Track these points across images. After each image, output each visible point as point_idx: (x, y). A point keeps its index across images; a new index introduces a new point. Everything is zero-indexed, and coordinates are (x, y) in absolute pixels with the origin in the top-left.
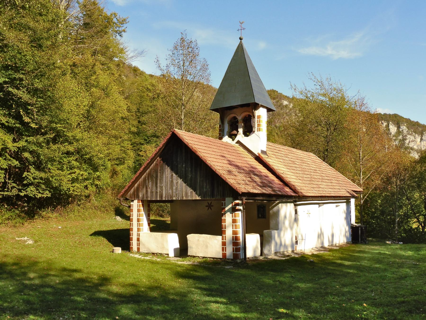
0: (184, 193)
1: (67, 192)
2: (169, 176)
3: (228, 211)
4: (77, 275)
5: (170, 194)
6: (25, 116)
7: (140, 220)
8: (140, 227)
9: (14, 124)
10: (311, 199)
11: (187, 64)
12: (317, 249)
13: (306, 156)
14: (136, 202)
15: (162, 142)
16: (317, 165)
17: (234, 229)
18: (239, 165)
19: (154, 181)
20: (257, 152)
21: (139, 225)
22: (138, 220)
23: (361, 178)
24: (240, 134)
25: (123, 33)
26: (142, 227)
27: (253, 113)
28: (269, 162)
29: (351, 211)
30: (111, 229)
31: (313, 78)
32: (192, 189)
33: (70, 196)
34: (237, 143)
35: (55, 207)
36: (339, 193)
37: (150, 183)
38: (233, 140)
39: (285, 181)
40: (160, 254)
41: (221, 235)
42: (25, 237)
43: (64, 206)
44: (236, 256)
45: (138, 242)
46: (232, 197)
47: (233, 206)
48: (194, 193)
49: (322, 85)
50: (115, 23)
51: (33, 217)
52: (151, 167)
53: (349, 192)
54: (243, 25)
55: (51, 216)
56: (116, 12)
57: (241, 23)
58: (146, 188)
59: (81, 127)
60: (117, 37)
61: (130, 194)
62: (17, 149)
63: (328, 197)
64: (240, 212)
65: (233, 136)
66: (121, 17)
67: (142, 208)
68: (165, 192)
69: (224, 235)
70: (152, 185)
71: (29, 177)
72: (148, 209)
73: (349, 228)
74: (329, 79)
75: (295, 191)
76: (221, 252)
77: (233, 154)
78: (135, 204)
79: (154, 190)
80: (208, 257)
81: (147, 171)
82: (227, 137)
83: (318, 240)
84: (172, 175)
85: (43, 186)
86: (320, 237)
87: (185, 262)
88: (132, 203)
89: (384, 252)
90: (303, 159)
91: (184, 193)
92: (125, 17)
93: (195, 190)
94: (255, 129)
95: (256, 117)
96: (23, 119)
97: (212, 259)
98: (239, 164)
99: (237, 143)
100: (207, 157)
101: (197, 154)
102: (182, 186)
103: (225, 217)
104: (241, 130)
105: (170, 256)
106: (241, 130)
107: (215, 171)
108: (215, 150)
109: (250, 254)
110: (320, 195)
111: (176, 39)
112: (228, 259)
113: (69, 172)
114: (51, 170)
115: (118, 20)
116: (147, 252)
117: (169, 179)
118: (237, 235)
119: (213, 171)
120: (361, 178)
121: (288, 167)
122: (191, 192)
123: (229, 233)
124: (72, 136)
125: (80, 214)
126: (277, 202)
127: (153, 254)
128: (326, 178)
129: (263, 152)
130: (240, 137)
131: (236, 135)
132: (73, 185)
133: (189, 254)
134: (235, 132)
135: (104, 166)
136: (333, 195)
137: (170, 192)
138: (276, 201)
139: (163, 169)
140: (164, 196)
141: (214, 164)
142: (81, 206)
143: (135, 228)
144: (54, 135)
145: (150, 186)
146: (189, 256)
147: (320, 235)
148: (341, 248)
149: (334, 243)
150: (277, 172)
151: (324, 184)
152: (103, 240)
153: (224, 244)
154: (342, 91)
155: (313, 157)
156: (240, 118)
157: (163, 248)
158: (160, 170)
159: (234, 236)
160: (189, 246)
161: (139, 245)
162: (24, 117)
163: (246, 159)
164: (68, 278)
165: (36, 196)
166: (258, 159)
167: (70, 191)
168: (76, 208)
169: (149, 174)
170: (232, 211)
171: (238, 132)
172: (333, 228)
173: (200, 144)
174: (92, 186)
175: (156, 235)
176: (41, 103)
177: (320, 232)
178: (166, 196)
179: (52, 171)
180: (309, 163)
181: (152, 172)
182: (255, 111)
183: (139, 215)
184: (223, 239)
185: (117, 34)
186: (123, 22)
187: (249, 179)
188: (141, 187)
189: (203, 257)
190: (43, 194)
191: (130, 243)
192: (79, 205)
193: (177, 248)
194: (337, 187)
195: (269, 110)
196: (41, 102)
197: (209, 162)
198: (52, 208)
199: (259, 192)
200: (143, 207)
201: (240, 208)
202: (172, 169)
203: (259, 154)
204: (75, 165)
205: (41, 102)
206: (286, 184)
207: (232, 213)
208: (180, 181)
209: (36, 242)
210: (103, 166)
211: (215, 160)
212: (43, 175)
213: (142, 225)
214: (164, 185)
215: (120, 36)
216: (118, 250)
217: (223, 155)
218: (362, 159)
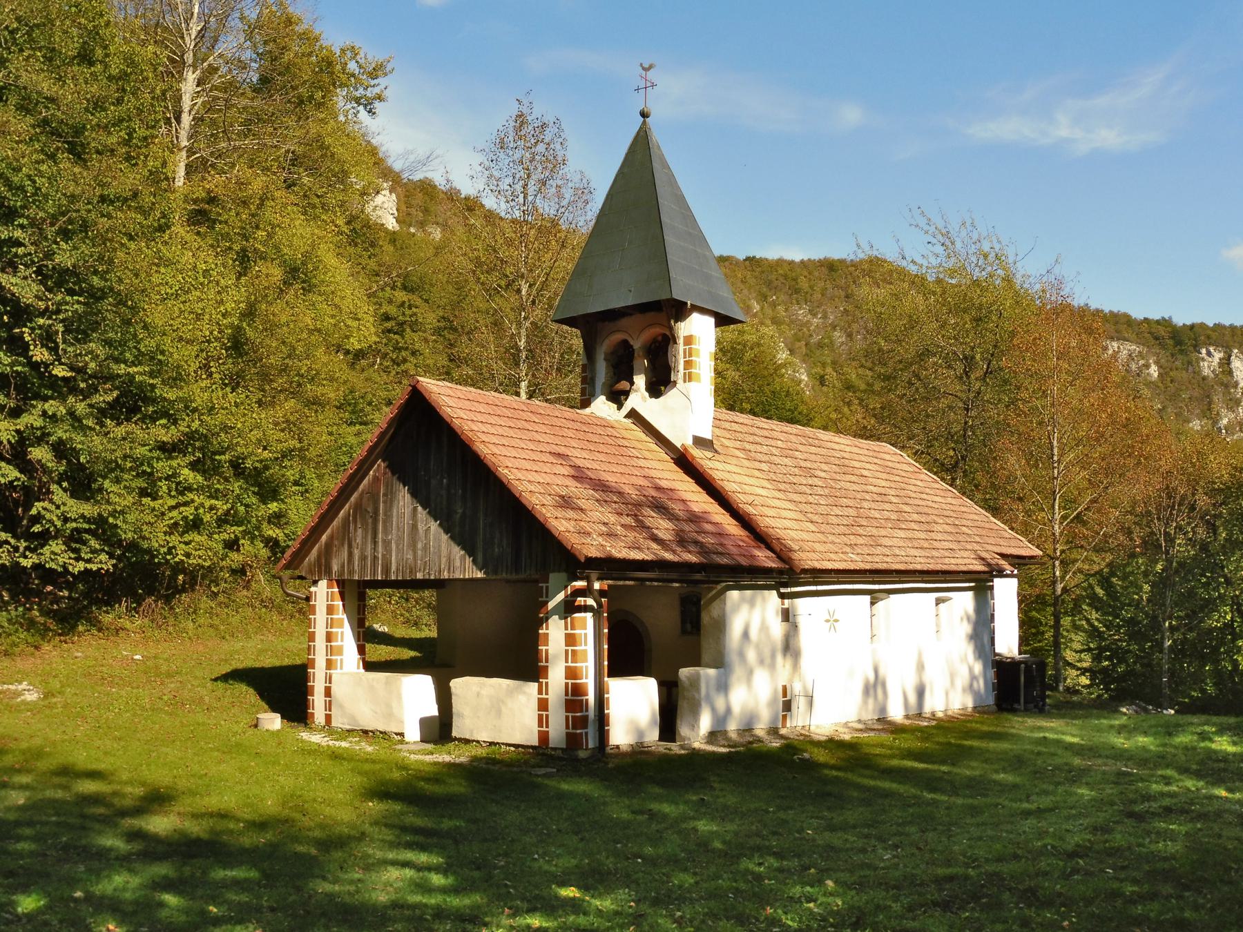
0: (444, 560)
1: (168, 557)
2: (408, 511)
3: (555, 611)
4: (89, 787)
5: (409, 562)
6: (36, 346)
7: (334, 637)
8: (333, 657)
9: (12, 365)
10: (834, 578)
11: (531, 189)
12: (860, 726)
13: (866, 452)
14: (323, 584)
15: (382, 417)
16: (897, 478)
17: (570, 664)
18: (610, 479)
19: (370, 527)
20: (682, 439)
21: (331, 650)
22: (329, 637)
23: (1057, 516)
24: (636, 391)
25: (377, 104)
26: (339, 658)
27: (671, 329)
28: (710, 472)
29: (993, 616)
30: (286, 662)
31: (922, 222)
32: (463, 548)
33: (179, 568)
34: (627, 416)
35: (139, 601)
36: (946, 561)
37: (360, 531)
38: (620, 407)
39: (754, 525)
40: (381, 732)
41: (538, 681)
42: (20, 683)
43: (168, 599)
44: (573, 740)
45: (328, 699)
46: (566, 571)
47: (566, 597)
48: (469, 560)
49: (947, 240)
50: (353, 75)
51: (73, 628)
52: (361, 487)
53: (983, 559)
54: (651, 75)
55: (128, 625)
56: (357, 45)
57: (644, 69)
58: (350, 546)
59: (214, 376)
60: (359, 115)
61: (310, 564)
62: (14, 437)
63: (936, 572)
64: (589, 616)
65: (618, 397)
66: (370, 58)
67: (341, 603)
68: (397, 556)
69: (544, 681)
70: (365, 538)
71: (48, 516)
72: (359, 605)
73: (985, 667)
74: (968, 224)
75: (782, 554)
76: (535, 728)
77: (602, 448)
78: (323, 592)
79: (369, 552)
80: (503, 744)
81: (353, 499)
82: (603, 398)
83: (865, 702)
84: (415, 509)
85: (94, 543)
86: (872, 692)
87: (444, 756)
88: (313, 589)
89: (1056, 736)
90: (847, 462)
91: (444, 560)
92: (380, 58)
93: (470, 550)
94: (679, 375)
95: (681, 341)
96: (31, 353)
97: (512, 749)
98: (610, 479)
99: (627, 416)
100: (501, 458)
101: (475, 448)
102: (440, 540)
103: (547, 629)
104: (640, 381)
105: (407, 739)
106: (640, 381)
107: (517, 495)
108: (538, 437)
109: (620, 737)
110: (868, 567)
111: (502, 118)
112: (552, 748)
113: (172, 502)
114: (111, 495)
115: (360, 67)
116: (348, 727)
117: (407, 519)
118: (578, 681)
119: (514, 496)
120: (1057, 516)
121: (782, 486)
122: (463, 559)
123: (556, 677)
124: (180, 399)
125: (216, 621)
126: (719, 587)
127: (366, 732)
128: (915, 517)
129: (699, 442)
130: (639, 399)
131: (626, 394)
132: (187, 538)
133: (454, 734)
134: (624, 385)
135: (301, 485)
136: (919, 567)
137: (410, 556)
138: (718, 582)
139: (392, 492)
140: (394, 568)
141: (520, 475)
142: (221, 598)
143: (320, 661)
144: (115, 393)
145: (359, 540)
146: (456, 739)
147: (874, 687)
148: (947, 725)
149: (927, 709)
150: (731, 501)
151: (902, 534)
152: (248, 694)
153: (543, 705)
154: (1003, 258)
155: (887, 457)
156: (637, 344)
157: (390, 715)
158: (385, 495)
159: (570, 682)
160: (454, 710)
161: (329, 706)
162: (32, 347)
163: (642, 463)
164: (59, 794)
165: (70, 568)
166: (683, 461)
167: (177, 554)
168: (205, 603)
169: (358, 507)
170: (565, 613)
171: (632, 383)
172: (921, 667)
173: (492, 420)
174: (252, 543)
175: (373, 680)
176: (76, 306)
177: (872, 678)
178: (398, 570)
179: (113, 498)
180: (865, 473)
181: (365, 500)
182: (676, 322)
183: (331, 623)
184: (540, 692)
185: (361, 108)
186: (376, 72)
187: (629, 521)
188: (336, 542)
189: (491, 744)
190: (89, 561)
191: (306, 701)
192: (215, 595)
193: (431, 719)
194: (946, 543)
195: (722, 320)
196: (74, 305)
197: (506, 471)
198: (132, 603)
199: (648, 556)
200: (343, 599)
201: (588, 603)
202: (414, 494)
203: (685, 449)
204: (191, 481)
205: (74, 305)
206: (760, 537)
207: (566, 618)
208: (434, 526)
209: (48, 695)
210: (296, 483)
211: (528, 465)
212: (88, 509)
213: (340, 651)
214: (393, 536)
215: (369, 112)
216: (273, 721)
217: (562, 450)
218: (1059, 461)
